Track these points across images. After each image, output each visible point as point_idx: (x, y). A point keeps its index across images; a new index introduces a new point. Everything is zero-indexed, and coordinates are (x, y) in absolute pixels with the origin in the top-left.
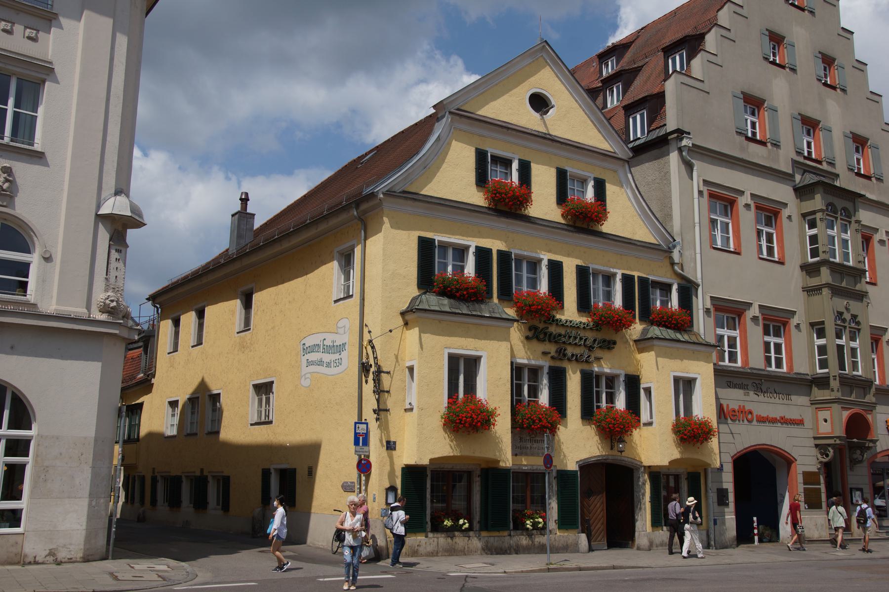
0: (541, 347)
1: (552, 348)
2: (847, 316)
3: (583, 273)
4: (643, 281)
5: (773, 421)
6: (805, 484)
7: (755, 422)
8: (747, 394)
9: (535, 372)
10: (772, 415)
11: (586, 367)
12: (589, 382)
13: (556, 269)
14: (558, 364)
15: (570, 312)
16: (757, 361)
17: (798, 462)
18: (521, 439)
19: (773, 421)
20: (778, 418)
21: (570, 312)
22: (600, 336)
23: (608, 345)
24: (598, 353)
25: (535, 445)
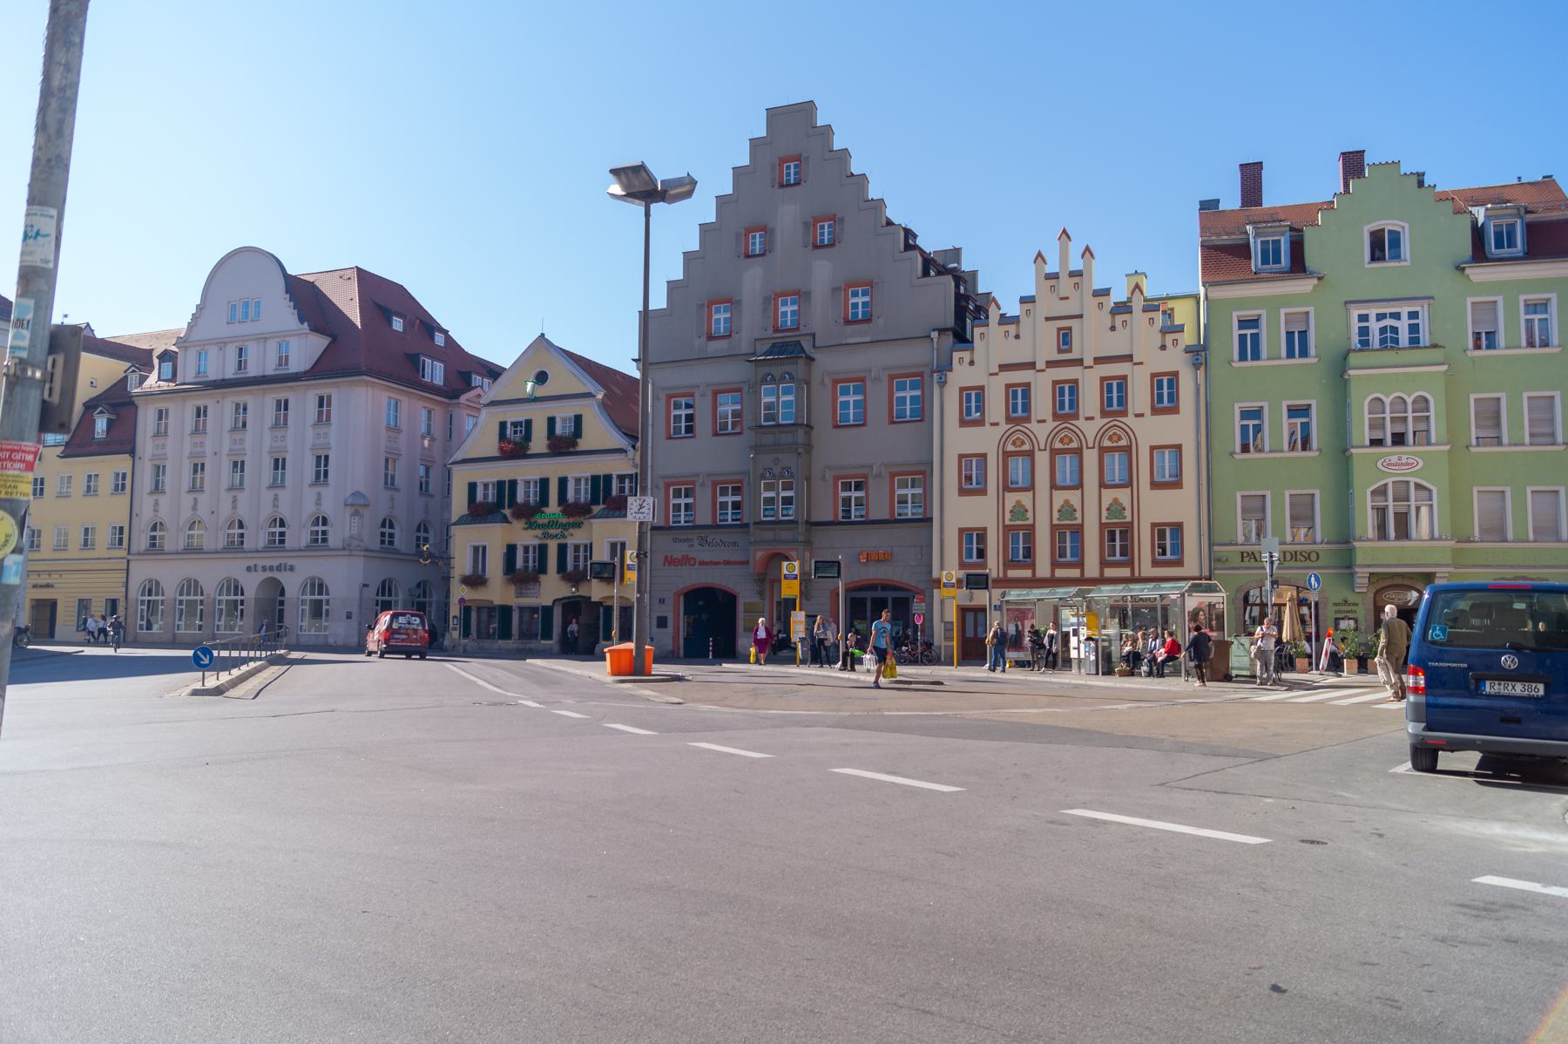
0: (531, 533)
1: (539, 532)
2: (777, 470)
3: (563, 482)
4: (608, 478)
5: (717, 563)
6: (745, 612)
7: (697, 566)
8: (692, 546)
9: (534, 547)
10: (714, 560)
11: (562, 541)
12: (562, 549)
13: (544, 483)
14: (544, 542)
15: (553, 507)
16: (703, 517)
17: (740, 595)
18: (521, 589)
19: (717, 563)
20: (721, 561)
21: (553, 507)
22: (571, 520)
23: (579, 525)
24: (571, 530)
25: (529, 591)
